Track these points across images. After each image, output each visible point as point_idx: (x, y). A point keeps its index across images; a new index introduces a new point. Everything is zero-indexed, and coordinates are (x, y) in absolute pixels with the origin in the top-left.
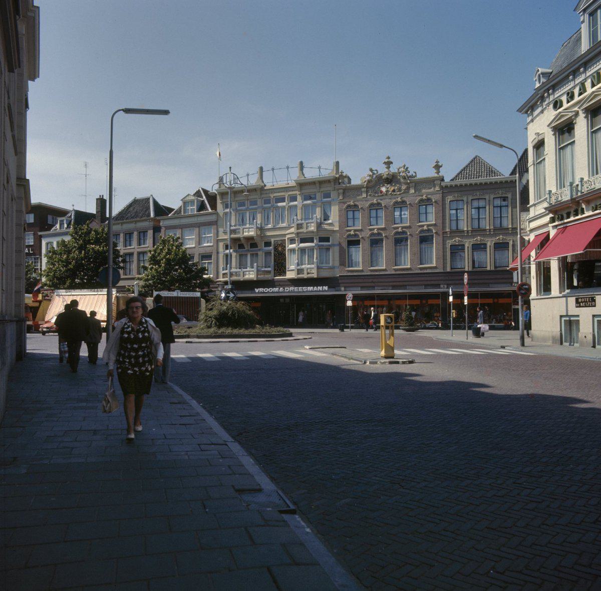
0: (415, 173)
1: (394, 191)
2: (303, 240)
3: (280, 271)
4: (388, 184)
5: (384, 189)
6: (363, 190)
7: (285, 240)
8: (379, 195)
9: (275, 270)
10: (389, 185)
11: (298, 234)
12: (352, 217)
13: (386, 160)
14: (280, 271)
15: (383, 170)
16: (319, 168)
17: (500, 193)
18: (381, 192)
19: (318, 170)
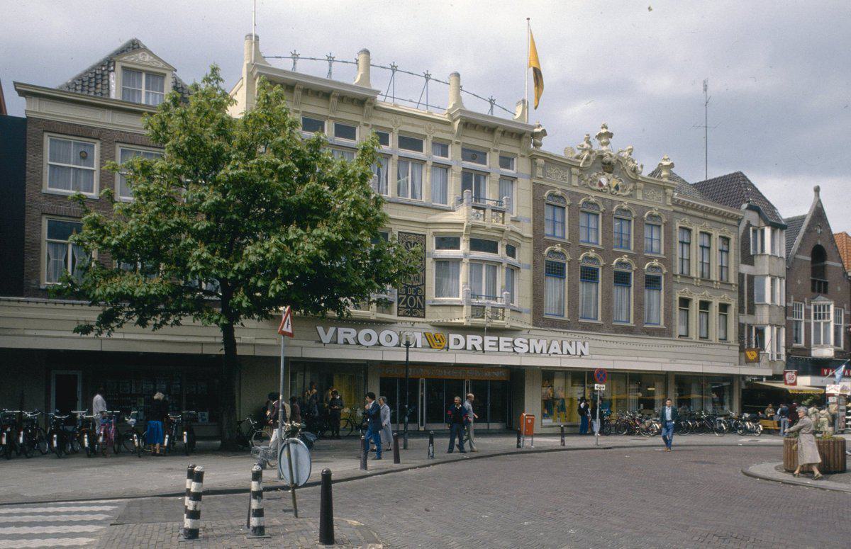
0: (642, 166)
1: (617, 188)
2: (476, 244)
3: (412, 304)
4: (610, 173)
5: (604, 180)
6: (574, 170)
7: (425, 235)
8: (597, 187)
9: (399, 300)
10: (611, 175)
11: (473, 227)
12: (550, 218)
13: (604, 131)
14: (412, 304)
15: (597, 146)
16: (492, 102)
17: (726, 231)
18: (601, 184)
19: (489, 105)
